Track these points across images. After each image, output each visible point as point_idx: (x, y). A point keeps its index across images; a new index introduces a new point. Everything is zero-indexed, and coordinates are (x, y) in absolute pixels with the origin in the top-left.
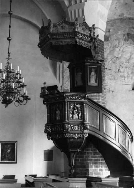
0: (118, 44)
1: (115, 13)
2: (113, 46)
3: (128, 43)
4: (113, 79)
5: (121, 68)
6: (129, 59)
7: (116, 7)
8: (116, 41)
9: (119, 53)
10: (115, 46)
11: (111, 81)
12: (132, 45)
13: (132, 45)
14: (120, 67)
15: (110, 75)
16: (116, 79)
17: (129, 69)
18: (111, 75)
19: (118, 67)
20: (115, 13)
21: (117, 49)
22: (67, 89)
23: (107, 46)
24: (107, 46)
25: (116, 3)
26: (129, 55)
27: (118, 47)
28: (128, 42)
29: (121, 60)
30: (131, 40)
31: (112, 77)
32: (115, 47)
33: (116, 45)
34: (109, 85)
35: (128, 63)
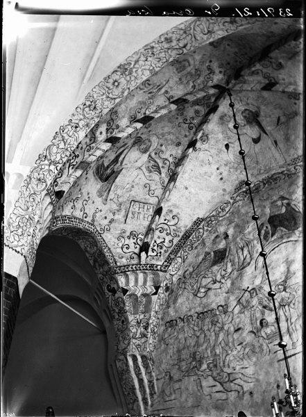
0: (248, 256)
1: (224, 190)
2: (237, 267)
3: (273, 242)
4: (250, 353)
5: (267, 312)
6: (285, 281)
7: (221, 176)
8: (242, 250)
9: (256, 277)
10: (243, 264)
11: (246, 363)
12: (284, 241)
13: (284, 241)
14: (263, 314)
15: (240, 346)
16: (257, 350)
17: (292, 305)
18: (241, 343)
19: (258, 315)
20: (224, 190)
21: (249, 270)
23: (223, 273)
24: (223, 273)
25: (218, 169)
26: (283, 268)
27: (249, 264)
28: (275, 237)
29: (263, 291)
30: (282, 228)
31: (247, 350)
32: (242, 268)
33: (244, 259)
34: (240, 375)
35: (285, 290)
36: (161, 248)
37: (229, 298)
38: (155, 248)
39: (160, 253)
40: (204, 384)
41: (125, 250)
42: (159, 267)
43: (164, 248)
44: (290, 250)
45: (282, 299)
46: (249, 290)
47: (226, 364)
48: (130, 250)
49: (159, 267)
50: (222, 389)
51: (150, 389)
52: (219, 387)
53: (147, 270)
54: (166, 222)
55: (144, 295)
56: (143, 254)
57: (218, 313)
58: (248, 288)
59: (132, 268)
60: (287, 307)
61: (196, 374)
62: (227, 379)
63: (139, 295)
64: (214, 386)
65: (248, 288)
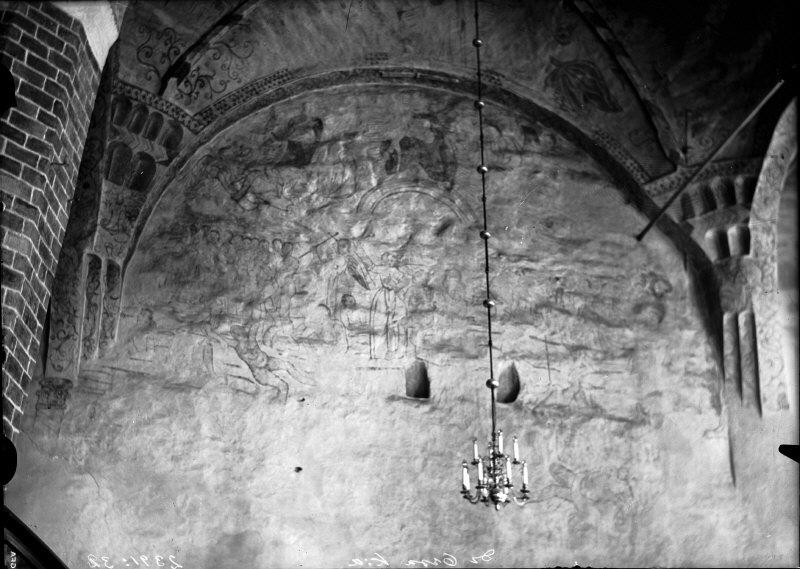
12: (418, 189)
13: (418, 189)
22: (62, 375)
36: (202, 86)
37: (298, 234)
38: (193, 80)
39: (197, 93)
40: (218, 356)
41: (142, 55)
42: (187, 119)
43: (207, 90)
44: (422, 207)
45: (389, 279)
46: (337, 237)
47: (268, 339)
48: (150, 61)
49: (187, 119)
50: (249, 375)
51: (104, 327)
52: (245, 371)
53: (166, 113)
54: (232, 44)
55: (143, 156)
56: (173, 81)
57: (271, 250)
58: (337, 234)
59: (144, 97)
60: (392, 292)
61: (206, 335)
62: (263, 364)
63: (135, 152)
64: (238, 366)
65: (337, 234)
